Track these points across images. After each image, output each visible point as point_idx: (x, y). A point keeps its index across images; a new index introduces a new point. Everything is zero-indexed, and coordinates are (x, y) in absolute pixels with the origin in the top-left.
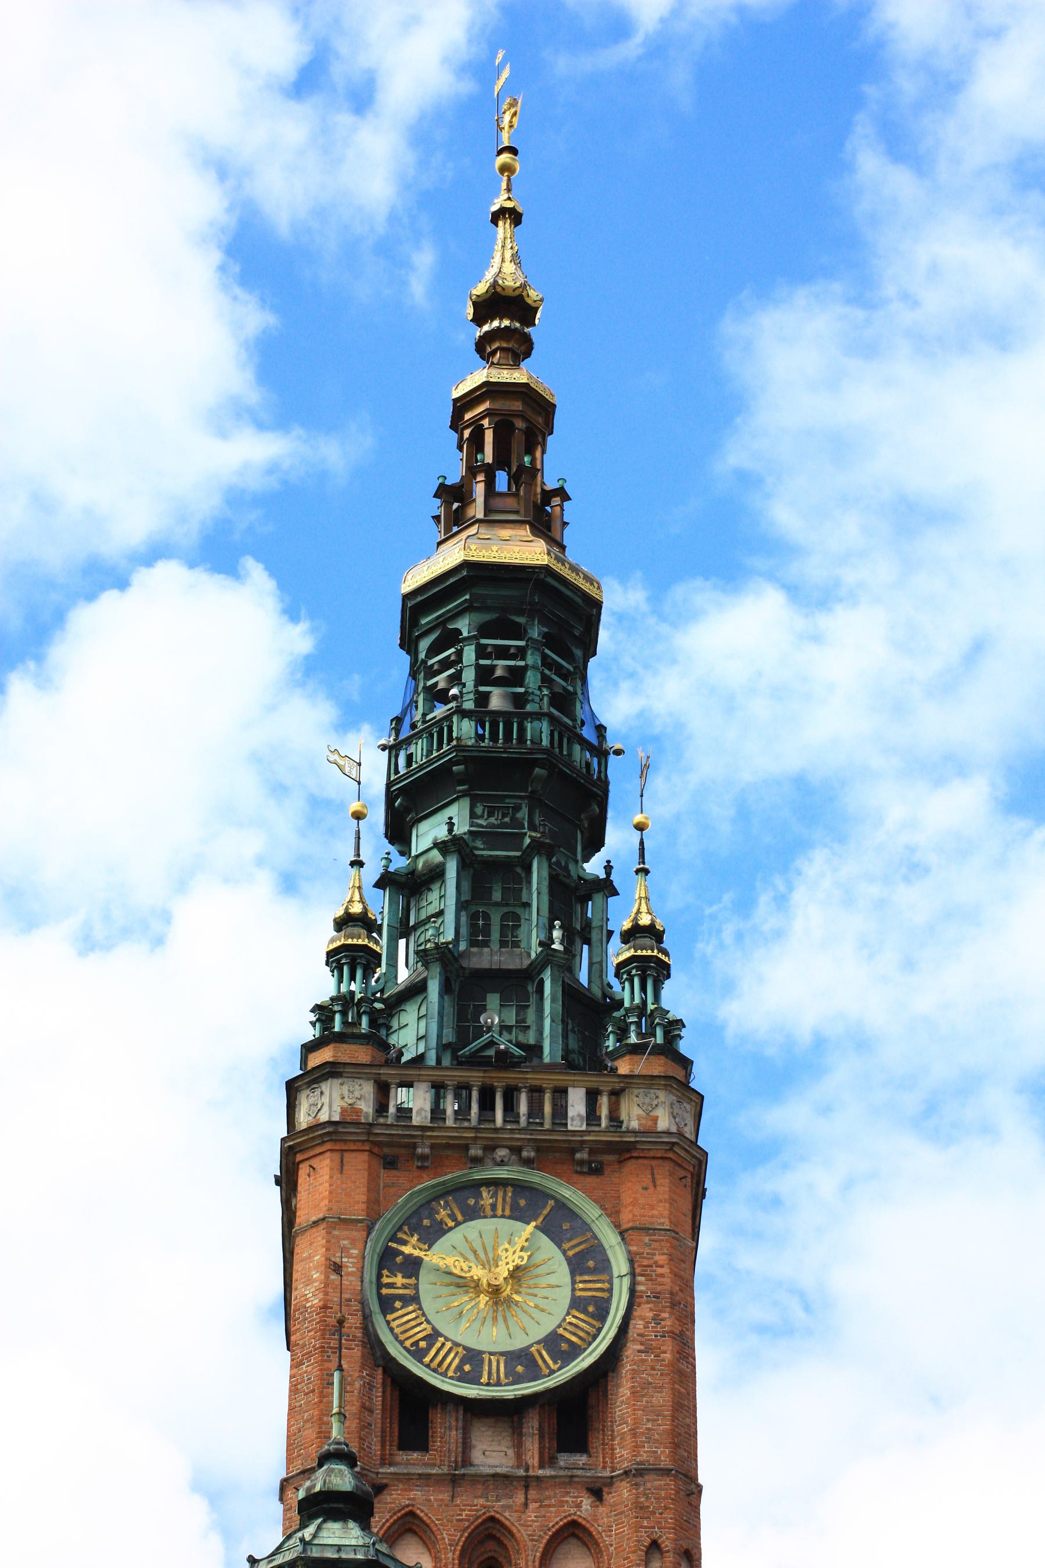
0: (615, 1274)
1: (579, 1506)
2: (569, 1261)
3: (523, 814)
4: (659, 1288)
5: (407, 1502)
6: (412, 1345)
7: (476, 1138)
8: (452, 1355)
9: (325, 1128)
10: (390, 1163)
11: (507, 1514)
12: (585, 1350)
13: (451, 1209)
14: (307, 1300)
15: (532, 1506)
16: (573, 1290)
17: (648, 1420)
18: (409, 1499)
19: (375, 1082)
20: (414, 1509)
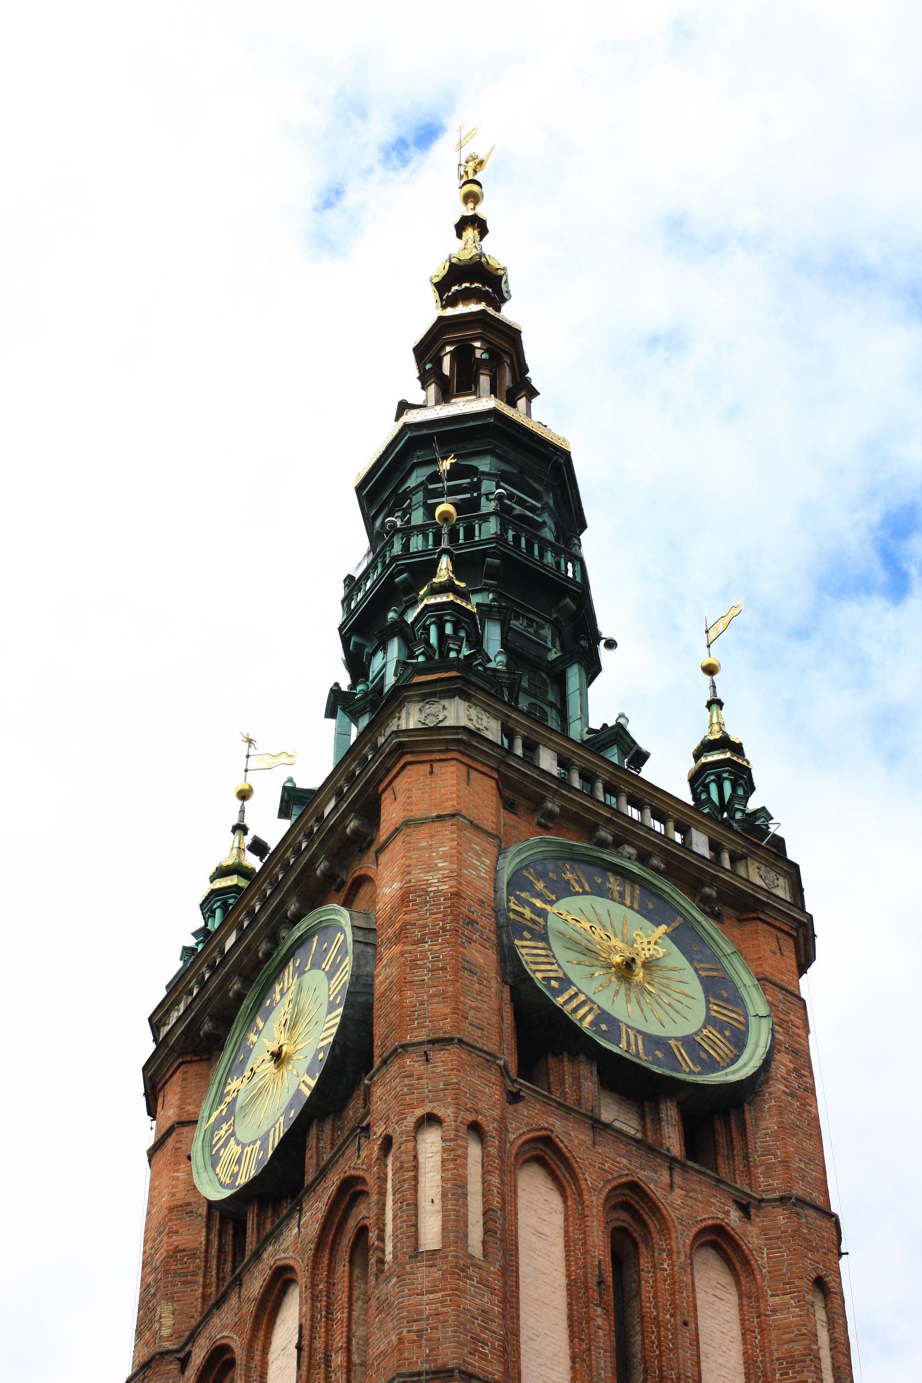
0: (752, 1012)
1: (727, 1213)
2: (702, 980)
3: (547, 632)
4: (797, 1046)
5: (546, 1125)
6: (543, 978)
7: (609, 820)
8: (586, 1008)
9: (458, 734)
10: (510, 806)
11: (652, 1186)
12: (724, 1068)
13: (578, 877)
14: (430, 885)
15: (677, 1191)
16: (708, 1009)
17: (801, 1160)
18: (547, 1123)
19: (502, 725)
20: (553, 1136)
